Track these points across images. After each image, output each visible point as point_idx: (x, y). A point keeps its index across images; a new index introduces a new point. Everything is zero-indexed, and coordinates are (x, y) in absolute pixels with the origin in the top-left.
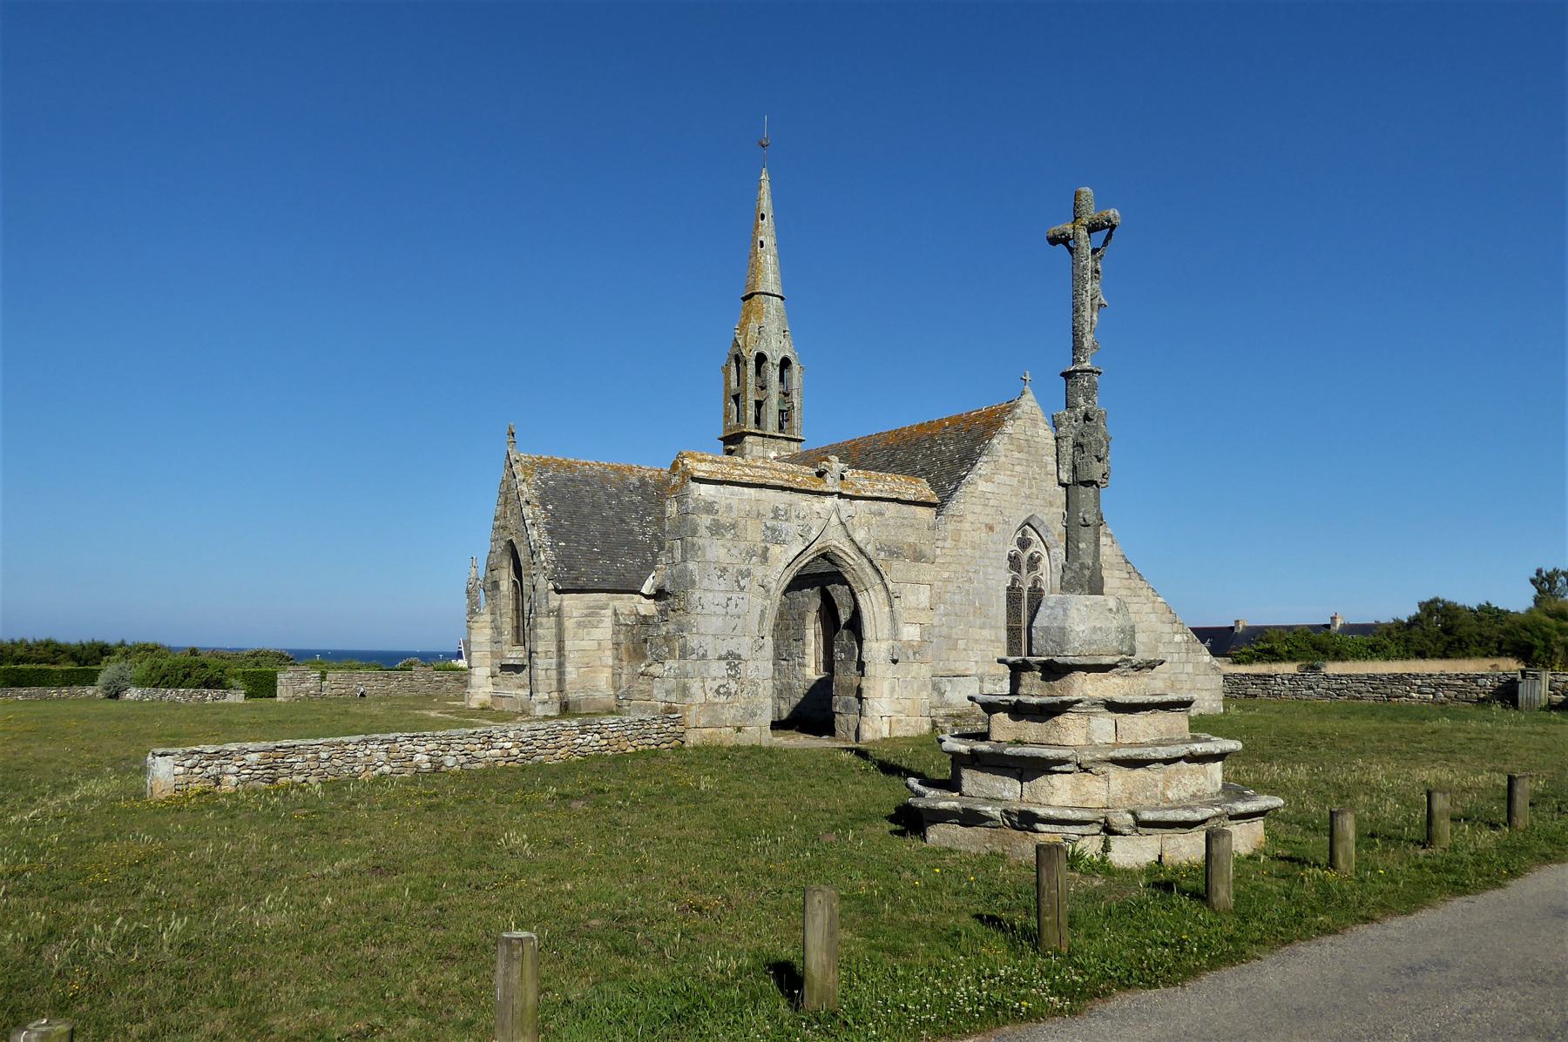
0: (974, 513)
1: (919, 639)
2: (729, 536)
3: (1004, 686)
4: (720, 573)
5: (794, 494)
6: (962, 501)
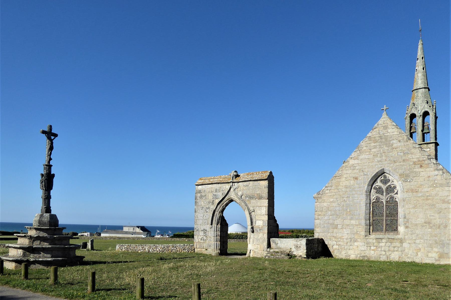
0: (347, 174)
1: (262, 225)
2: (204, 198)
3: (302, 242)
4: (201, 208)
5: (222, 184)
6: (341, 170)
